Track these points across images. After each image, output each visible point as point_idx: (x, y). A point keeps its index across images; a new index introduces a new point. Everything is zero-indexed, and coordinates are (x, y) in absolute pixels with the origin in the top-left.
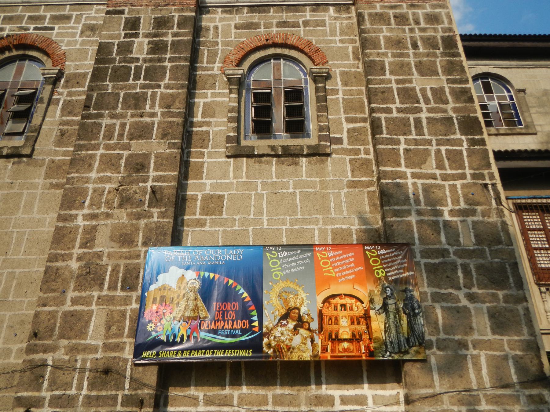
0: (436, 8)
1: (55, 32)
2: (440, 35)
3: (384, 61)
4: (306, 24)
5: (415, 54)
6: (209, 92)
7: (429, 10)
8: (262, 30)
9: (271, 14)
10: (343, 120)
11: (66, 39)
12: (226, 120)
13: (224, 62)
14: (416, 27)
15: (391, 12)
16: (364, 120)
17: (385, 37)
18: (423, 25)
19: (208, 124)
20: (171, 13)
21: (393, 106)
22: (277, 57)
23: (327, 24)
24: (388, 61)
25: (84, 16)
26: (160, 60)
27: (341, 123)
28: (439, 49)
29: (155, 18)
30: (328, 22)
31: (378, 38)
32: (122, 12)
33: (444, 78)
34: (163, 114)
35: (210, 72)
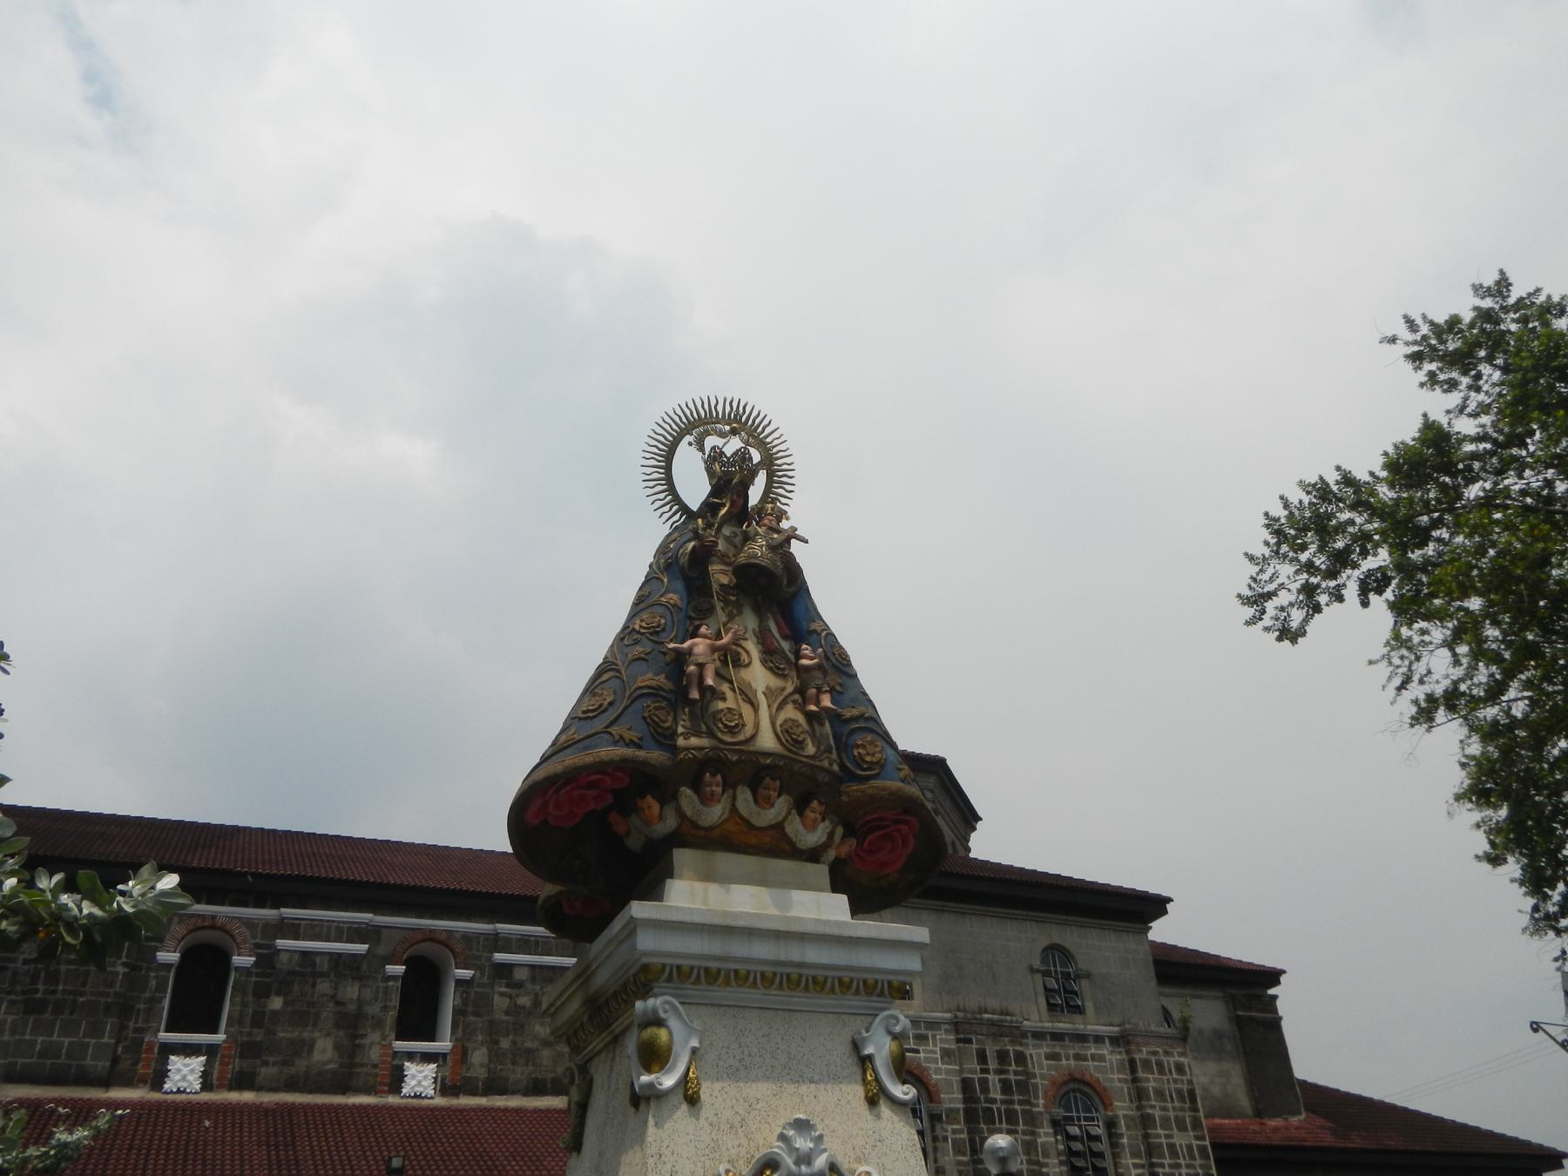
0: (1180, 1057)
1: (922, 1055)
2: (1185, 1087)
3: (1154, 1115)
4: (1094, 1057)
5: (1174, 1108)
6: (1041, 1130)
7: (1177, 1058)
8: (1064, 1062)
9: (1067, 1043)
10: (1131, 1166)
11: (933, 1066)
12: (1056, 1161)
13: (1045, 1098)
14: (1170, 1077)
15: (1153, 1059)
16: (1142, 1166)
17: (1154, 1088)
18: (1175, 1076)
19: (1046, 1165)
20: (1006, 1046)
21: (1165, 1162)
22: (1074, 1091)
23: (1107, 1058)
24: (1157, 1113)
25: (938, 1037)
26: (1012, 1102)
27: (1129, 1169)
28: (1186, 1103)
29: (997, 1051)
30: (1108, 1057)
31: (1148, 1088)
32: (969, 1041)
33: (1191, 1134)
34: (1030, 1162)
35: (1037, 1109)
